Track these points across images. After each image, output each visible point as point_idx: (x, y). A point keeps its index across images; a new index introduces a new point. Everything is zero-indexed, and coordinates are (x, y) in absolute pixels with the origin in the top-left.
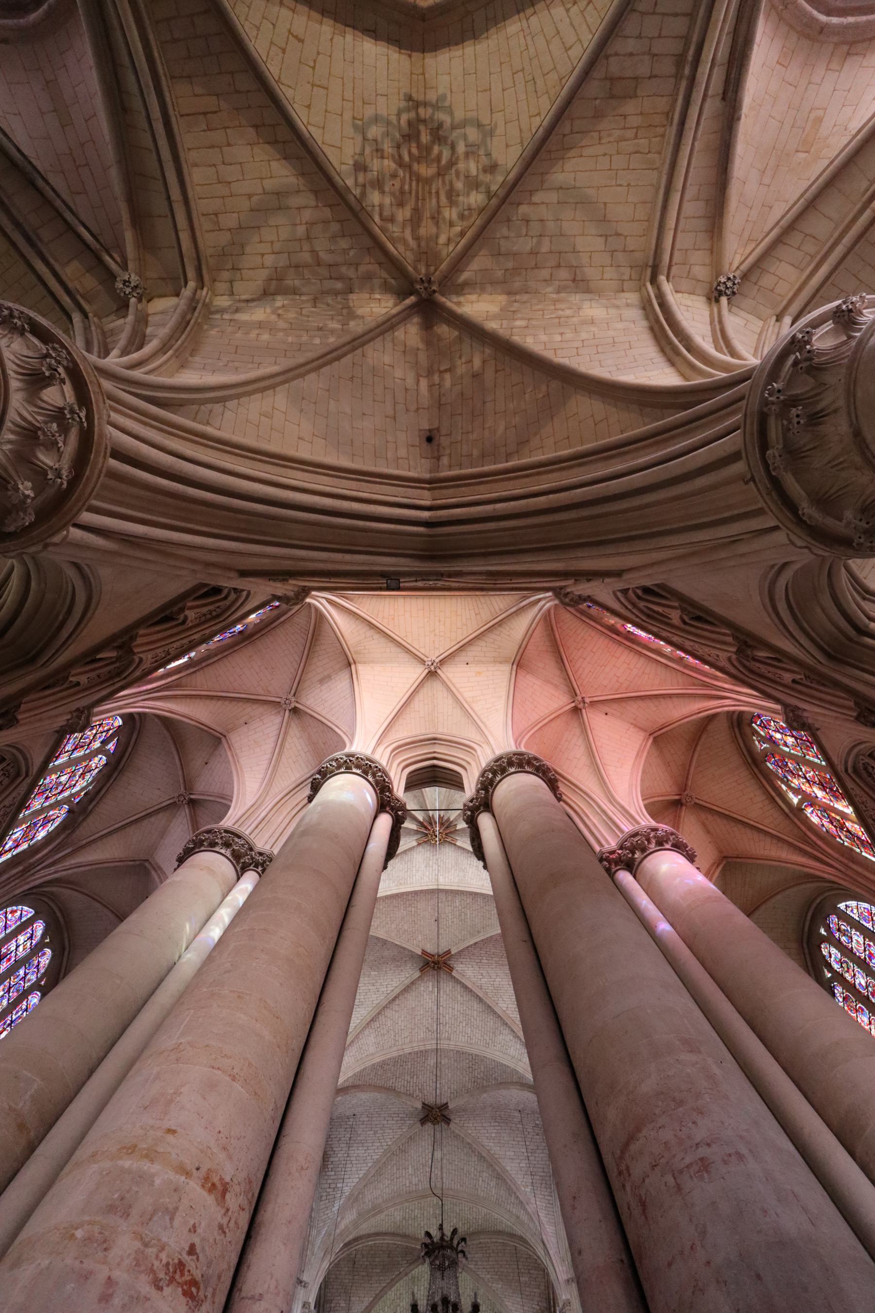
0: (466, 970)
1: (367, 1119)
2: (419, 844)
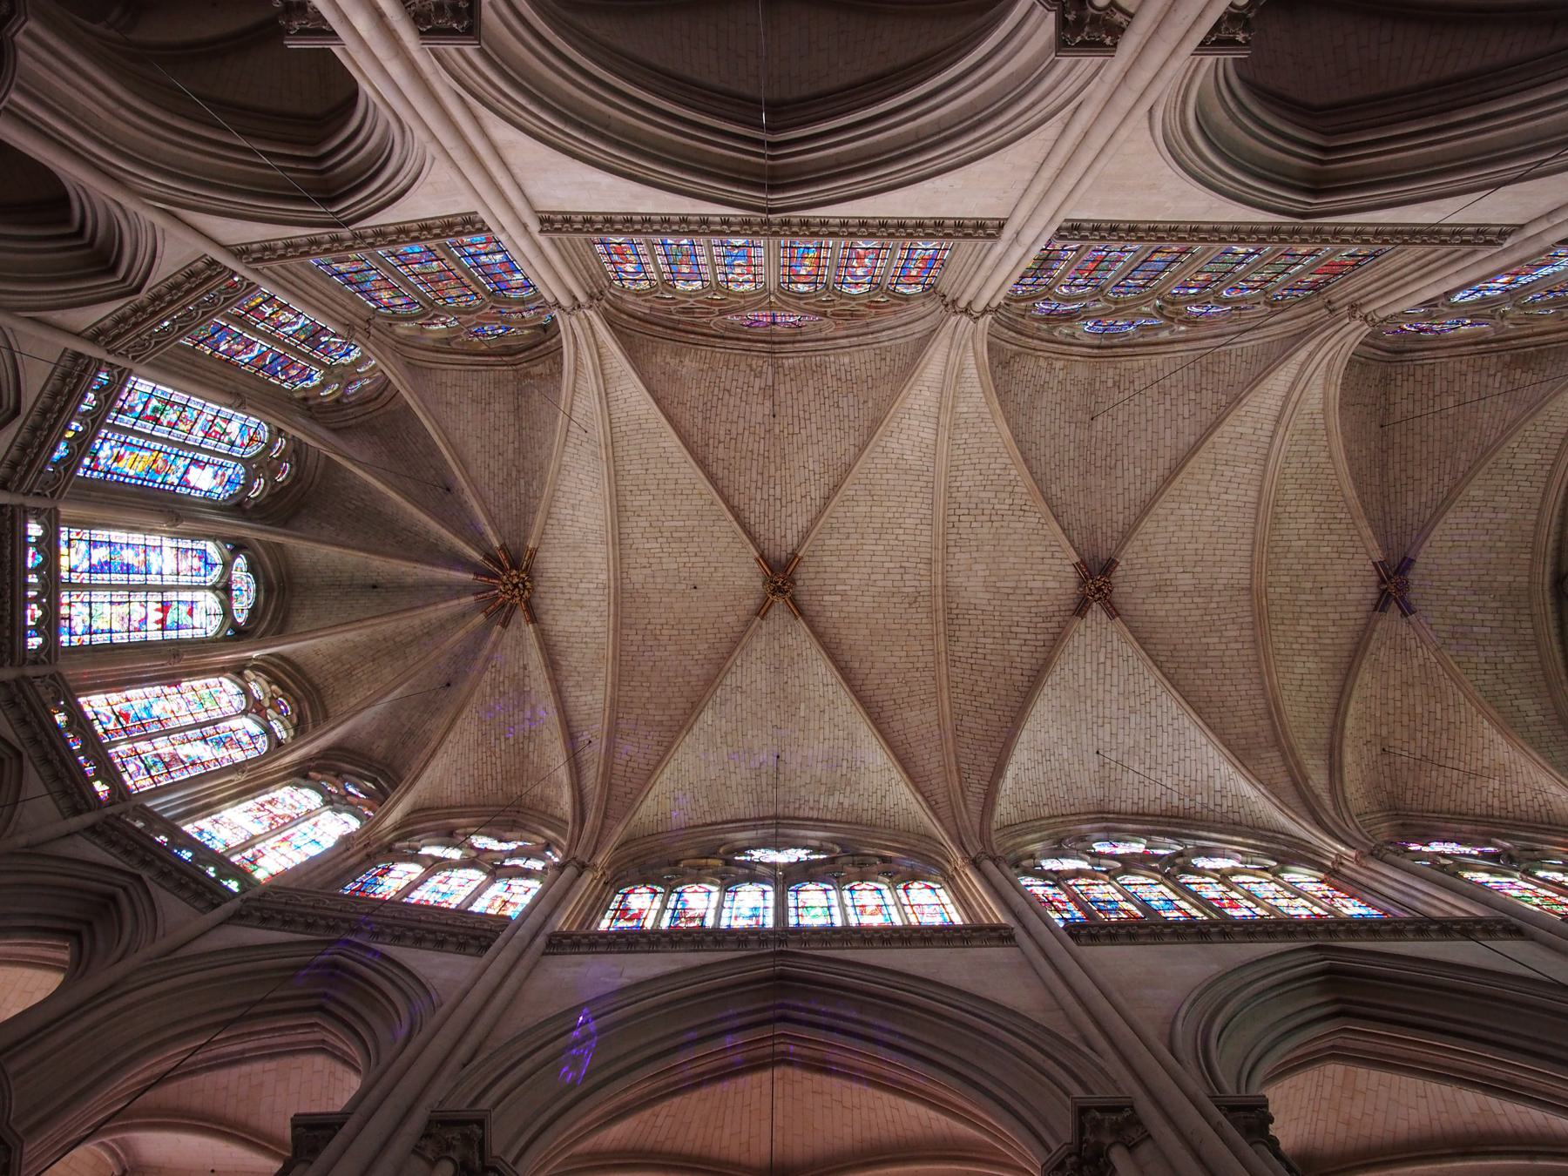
1: (1107, 726)
2: (533, 618)
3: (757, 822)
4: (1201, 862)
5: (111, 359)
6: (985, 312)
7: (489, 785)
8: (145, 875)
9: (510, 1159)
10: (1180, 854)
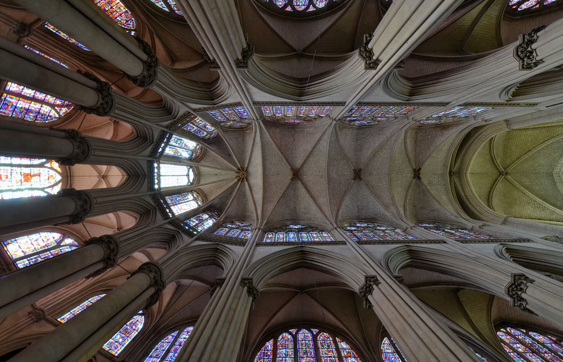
0: (298, 163)
2: (247, 181)
3: (291, 220)
4: (378, 228)
5: (169, 131)
6: (339, 120)
7: (239, 213)
8: (180, 231)
9: (256, 286)
10: (375, 227)
